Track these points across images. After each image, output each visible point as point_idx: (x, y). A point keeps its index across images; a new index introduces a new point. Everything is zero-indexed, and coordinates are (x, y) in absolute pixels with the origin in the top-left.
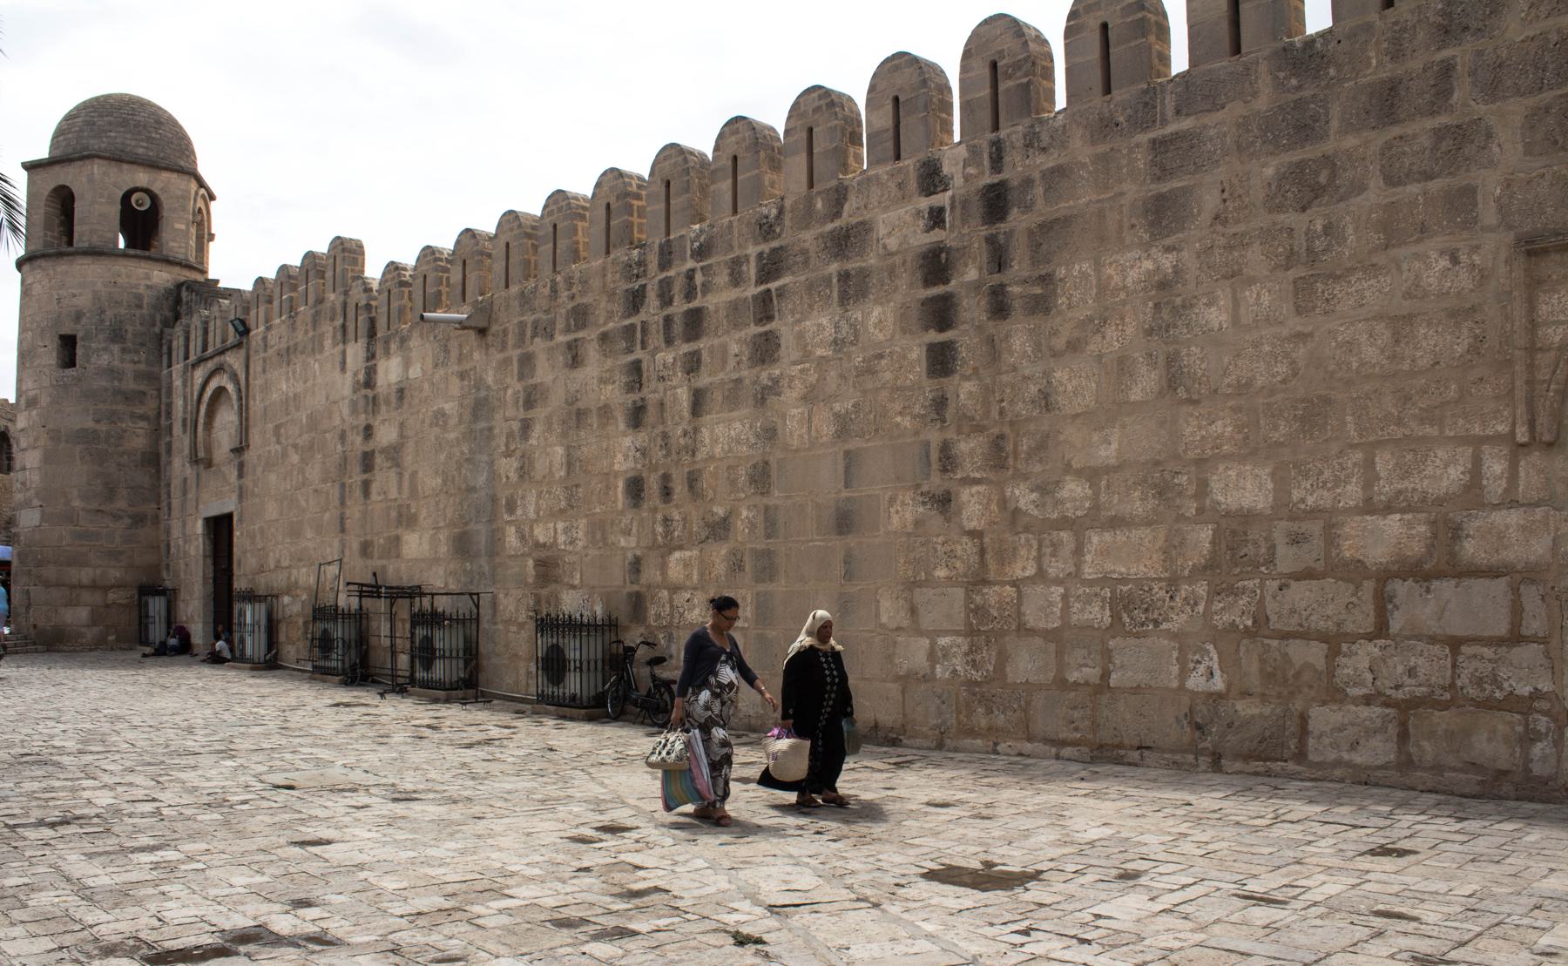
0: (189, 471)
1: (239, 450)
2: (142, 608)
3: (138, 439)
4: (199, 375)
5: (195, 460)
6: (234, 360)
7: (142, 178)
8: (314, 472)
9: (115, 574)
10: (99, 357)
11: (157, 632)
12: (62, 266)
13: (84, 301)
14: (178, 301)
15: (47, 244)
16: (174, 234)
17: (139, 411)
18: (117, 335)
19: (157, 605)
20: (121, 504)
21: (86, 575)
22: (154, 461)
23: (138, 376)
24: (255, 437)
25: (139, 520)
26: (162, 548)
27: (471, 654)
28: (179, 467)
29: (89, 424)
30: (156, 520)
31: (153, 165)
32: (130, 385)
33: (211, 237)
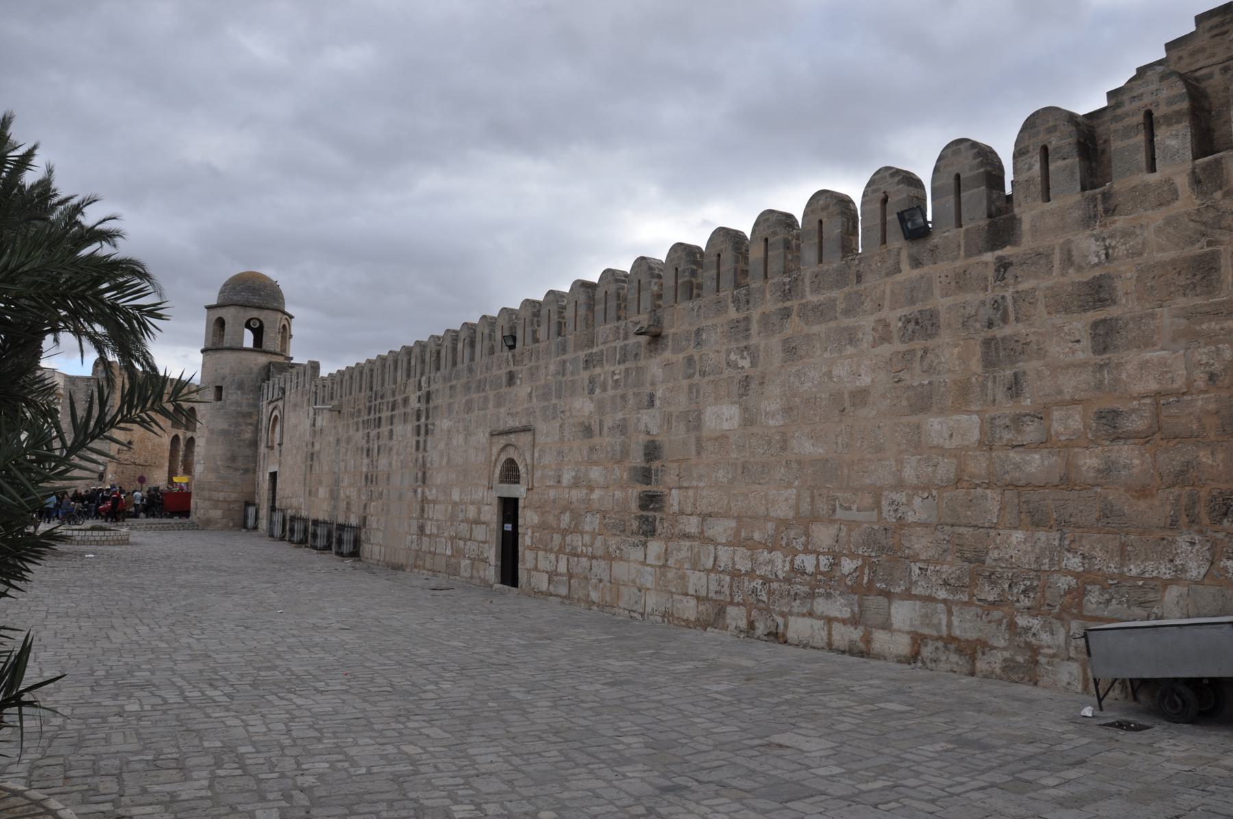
0: (266, 450)
1: (280, 445)
2: (246, 511)
3: (248, 435)
4: (271, 407)
5: (268, 447)
6: (280, 403)
7: (255, 313)
8: (299, 459)
9: (234, 496)
10: (231, 396)
11: (250, 522)
12: (218, 355)
13: (227, 371)
14: (269, 370)
15: (214, 344)
16: (271, 340)
17: (249, 421)
18: (240, 386)
19: (251, 510)
20: (240, 464)
21: (221, 496)
22: (254, 444)
23: (249, 405)
24: (285, 441)
25: (246, 471)
26: (255, 484)
27: (357, 542)
28: (262, 449)
29: (225, 426)
30: (254, 471)
31: (260, 308)
32: (245, 409)
33: (291, 336)
